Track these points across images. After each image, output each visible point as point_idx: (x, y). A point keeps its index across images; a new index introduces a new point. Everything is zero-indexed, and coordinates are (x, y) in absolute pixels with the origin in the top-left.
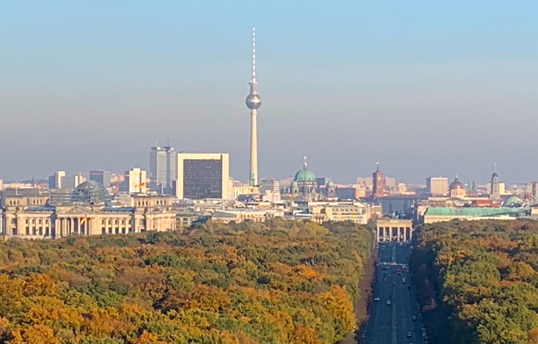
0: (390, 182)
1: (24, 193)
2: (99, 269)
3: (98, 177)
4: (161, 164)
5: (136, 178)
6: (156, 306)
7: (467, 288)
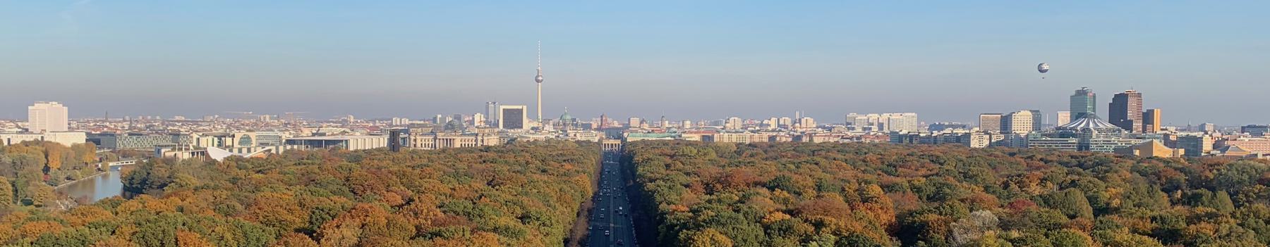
0: (609, 120)
1: (420, 126)
2: (459, 165)
3: (458, 118)
4: (491, 112)
5: (479, 118)
6: (489, 184)
7: (649, 175)
